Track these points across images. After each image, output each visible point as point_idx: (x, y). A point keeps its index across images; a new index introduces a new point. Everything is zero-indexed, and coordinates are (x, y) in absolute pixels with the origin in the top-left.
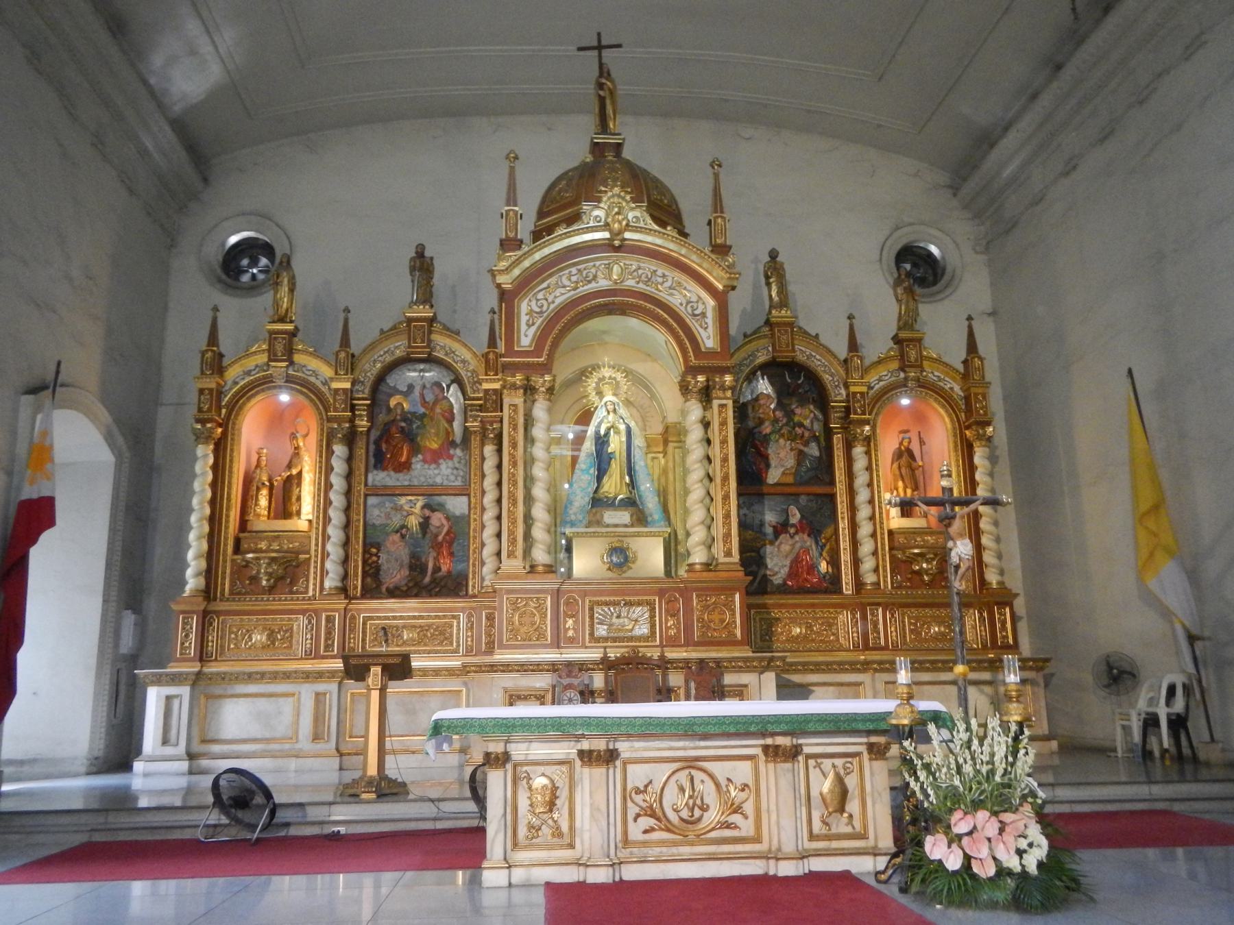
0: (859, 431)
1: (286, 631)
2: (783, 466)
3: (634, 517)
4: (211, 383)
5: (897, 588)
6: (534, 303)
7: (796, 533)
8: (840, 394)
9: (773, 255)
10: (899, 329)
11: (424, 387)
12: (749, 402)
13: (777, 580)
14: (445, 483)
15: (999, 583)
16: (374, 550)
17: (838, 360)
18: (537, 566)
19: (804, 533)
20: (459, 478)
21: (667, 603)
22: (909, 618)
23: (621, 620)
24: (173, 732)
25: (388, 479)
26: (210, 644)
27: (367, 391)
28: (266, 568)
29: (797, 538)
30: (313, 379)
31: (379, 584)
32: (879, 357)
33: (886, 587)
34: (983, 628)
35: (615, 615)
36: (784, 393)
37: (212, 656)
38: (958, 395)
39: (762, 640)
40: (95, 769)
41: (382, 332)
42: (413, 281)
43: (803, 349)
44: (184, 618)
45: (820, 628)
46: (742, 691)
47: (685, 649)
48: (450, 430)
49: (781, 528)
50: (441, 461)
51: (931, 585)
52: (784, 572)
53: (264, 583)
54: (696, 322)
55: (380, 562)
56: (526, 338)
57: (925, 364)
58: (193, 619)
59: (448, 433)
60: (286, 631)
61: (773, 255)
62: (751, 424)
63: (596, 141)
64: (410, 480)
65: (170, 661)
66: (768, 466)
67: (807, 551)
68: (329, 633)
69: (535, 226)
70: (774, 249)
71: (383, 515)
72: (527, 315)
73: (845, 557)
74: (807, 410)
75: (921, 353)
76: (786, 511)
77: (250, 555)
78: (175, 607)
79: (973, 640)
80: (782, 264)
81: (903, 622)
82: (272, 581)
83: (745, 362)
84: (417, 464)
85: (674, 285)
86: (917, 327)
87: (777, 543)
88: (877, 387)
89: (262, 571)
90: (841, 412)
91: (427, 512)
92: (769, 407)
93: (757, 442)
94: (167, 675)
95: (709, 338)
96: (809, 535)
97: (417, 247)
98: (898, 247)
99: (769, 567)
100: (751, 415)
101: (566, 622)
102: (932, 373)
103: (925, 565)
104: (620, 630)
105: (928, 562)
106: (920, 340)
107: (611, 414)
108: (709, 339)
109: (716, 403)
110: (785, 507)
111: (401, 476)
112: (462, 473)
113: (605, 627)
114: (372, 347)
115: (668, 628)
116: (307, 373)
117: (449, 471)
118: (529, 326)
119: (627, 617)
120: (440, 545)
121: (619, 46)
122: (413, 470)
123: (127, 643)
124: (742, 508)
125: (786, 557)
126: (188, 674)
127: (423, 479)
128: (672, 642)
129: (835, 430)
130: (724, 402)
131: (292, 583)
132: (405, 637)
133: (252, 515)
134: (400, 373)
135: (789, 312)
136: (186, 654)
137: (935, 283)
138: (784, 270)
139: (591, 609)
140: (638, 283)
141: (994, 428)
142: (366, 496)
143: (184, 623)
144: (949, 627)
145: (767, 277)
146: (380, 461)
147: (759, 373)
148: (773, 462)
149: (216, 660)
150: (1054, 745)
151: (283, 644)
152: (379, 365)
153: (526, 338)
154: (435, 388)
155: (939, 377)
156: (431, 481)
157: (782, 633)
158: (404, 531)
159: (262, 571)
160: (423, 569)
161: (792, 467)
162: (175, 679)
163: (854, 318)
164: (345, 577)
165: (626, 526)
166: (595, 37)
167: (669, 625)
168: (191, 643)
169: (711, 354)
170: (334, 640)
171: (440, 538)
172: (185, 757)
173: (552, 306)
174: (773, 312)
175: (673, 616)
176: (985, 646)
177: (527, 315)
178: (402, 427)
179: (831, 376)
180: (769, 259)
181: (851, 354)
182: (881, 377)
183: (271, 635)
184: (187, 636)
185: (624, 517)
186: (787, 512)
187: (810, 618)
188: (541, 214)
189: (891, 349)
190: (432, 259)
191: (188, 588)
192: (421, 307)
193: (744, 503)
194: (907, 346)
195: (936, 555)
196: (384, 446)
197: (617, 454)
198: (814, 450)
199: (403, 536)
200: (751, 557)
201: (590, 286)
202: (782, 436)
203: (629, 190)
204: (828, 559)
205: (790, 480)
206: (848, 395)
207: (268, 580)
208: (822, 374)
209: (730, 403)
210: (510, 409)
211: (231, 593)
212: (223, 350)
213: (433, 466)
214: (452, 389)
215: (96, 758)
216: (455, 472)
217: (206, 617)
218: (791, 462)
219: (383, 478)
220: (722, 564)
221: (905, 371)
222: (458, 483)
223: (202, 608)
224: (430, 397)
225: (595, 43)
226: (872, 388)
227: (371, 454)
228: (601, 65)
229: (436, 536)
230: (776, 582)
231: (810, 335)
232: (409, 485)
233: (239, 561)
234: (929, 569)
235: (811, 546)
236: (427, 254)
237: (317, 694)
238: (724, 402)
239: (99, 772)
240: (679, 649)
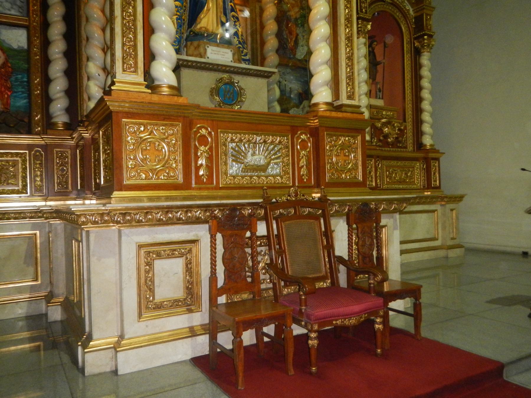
3: (236, 57)
51: (393, 145)
87: (302, 106)
101: (197, 158)
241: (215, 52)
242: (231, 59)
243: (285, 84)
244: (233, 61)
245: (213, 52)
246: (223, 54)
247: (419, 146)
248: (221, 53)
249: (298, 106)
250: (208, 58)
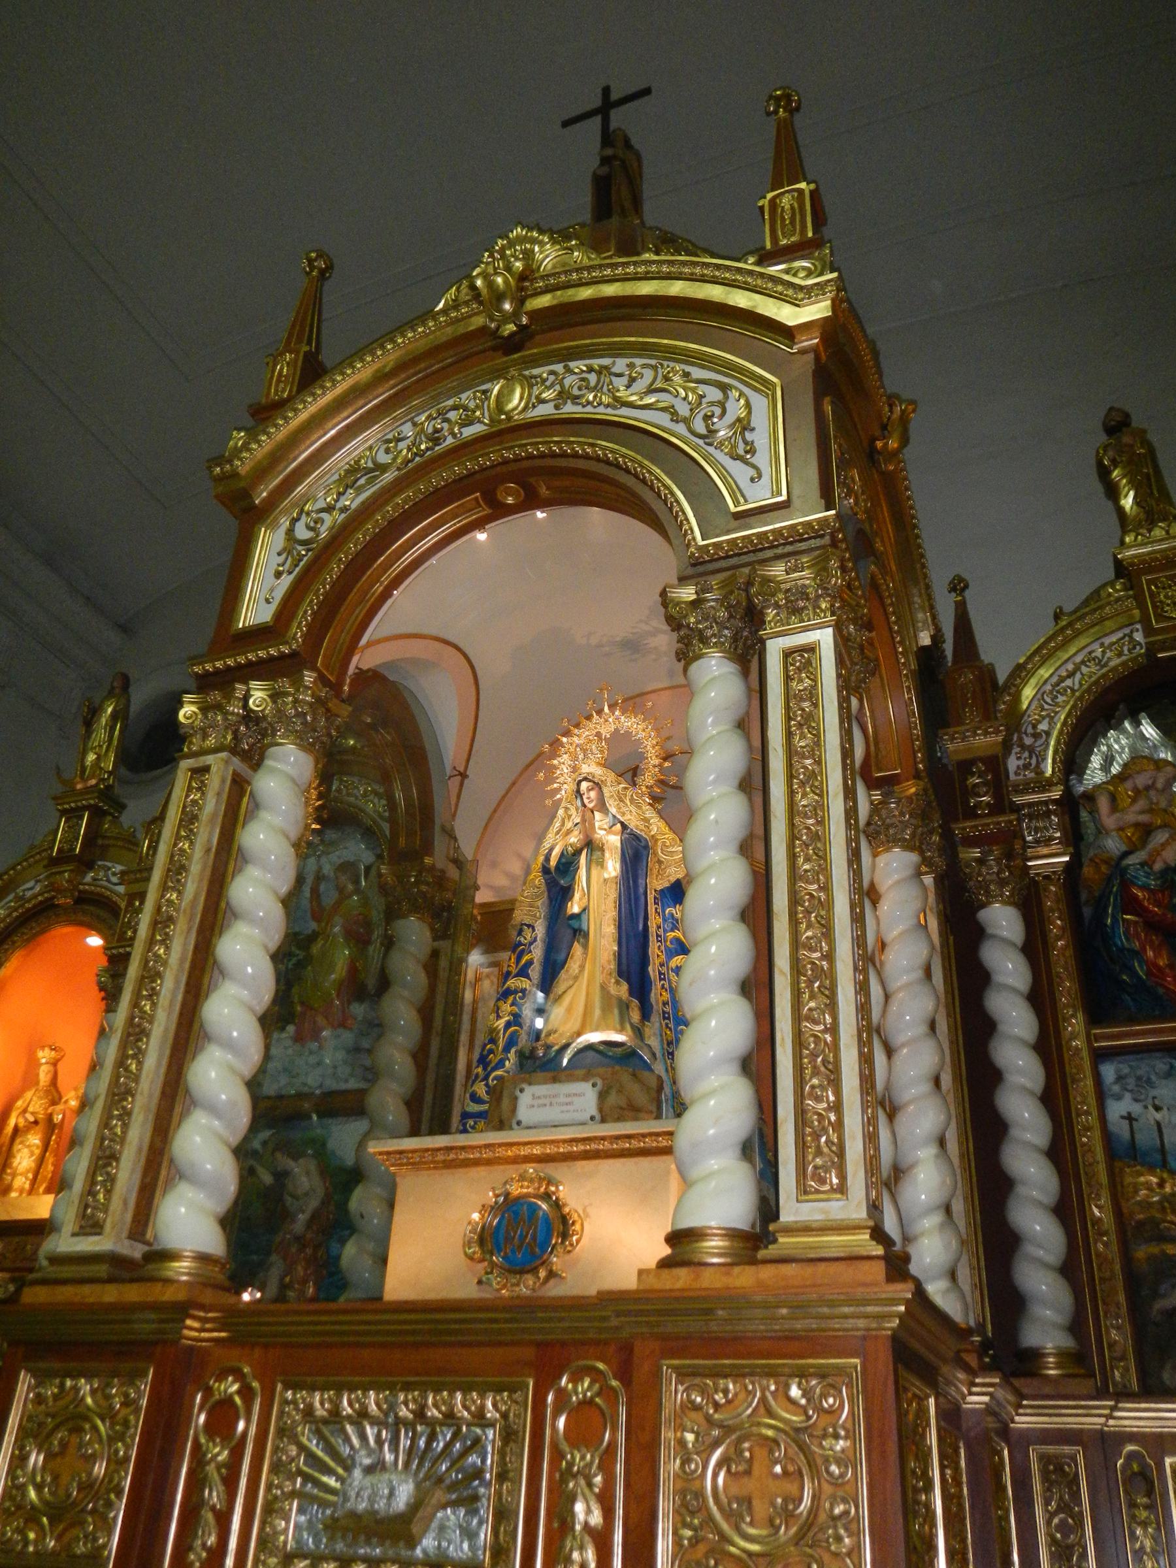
12: (1097, 787)
62: (1113, 845)
100: (1109, 821)
109: (775, 648)
124: (1119, 1098)
127: (283, 1080)
145: (1104, 473)
177: (279, 554)
193: (1120, 1078)
209: (825, 638)
220: (790, 1230)
241: (541, 1102)
242: (593, 1111)
243: (1159, 1124)
244: (598, 1117)
245: (536, 1102)
246: (568, 1100)
248: (562, 1099)
250: (519, 1123)
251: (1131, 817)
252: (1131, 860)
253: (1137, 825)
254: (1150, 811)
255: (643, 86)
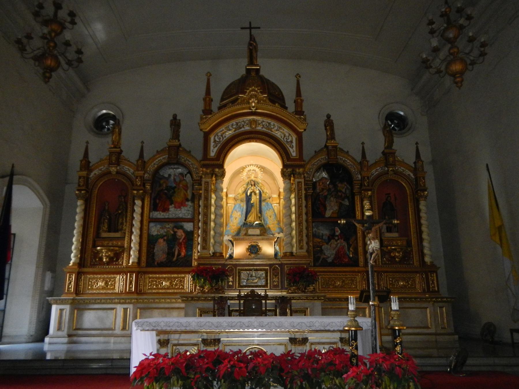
0: (366, 194)
1: (113, 281)
2: (333, 209)
3: (262, 232)
4: (84, 173)
5: (384, 264)
6: (216, 137)
7: (338, 239)
8: (358, 177)
9: (329, 116)
10: (385, 148)
11: (175, 175)
13: (330, 260)
14: (184, 217)
15: (431, 262)
16: (152, 246)
17: (357, 162)
18: (217, 253)
19: (341, 239)
20: (189, 215)
21: (273, 270)
22: (389, 278)
23: (253, 278)
24: (63, 325)
25: (159, 215)
26: (80, 286)
27: (150, 177)
28: (105, 254)
29: (339, 241)
30: (128, 172)
31: (153, 260)
32: (376, 161)
33: (379, 264)
34: (423, 283)
35: (250, 275)
36: (333, 177)
37: (81, 292)
38: (412, 177)
39: (322, 287)
40: (31, 340)
41: (157, 151)
42: (171, 130)
43: (341, 157)
44: (69, 275)
45: (348, 282)
46: (306, 311)
47: (280, 291)
48: (186, 194)
49: (332, 237)
50: (182, 207)
52: (332, 257)
53: (104, 260)
54: (288, 145)
55: (155, 251)
56: (213, 153)
57: (397, 163)
58: (73, 275)
59: (185, 195)
60: (113, 281)
61: (329, 116)
62: (318, 191)
63: (247, 67)
64: (168, 216)
65: (62, 294)
66: (325, 209)
67: (343, 247)
68: (131, 283)
69: (220, 105)
70: (328, 114)
71: (156, 230)
72: (213, 142)
73: (360, 249)
74: (344, 185)
75: (395, 158)
76: (334, 231)
77: (99, 248)
78: (65, 270)
79: (419, 288)
80: (332, 121)
81: (387, 280)
82: (108, 259)
83: (315, 164)
84: (172, 208)
85: (278, 129)
86: (393, 148)
87: (330, 244)
88: (375, 174)
89: (104, 255)
90: (359, 185)
91: (176, 230)
92: (326, 183)
93: (321, 199)
94: (60, 300)
95: (294, 151)
96: (344, 240)
97: (173, 116)
98: (387, 112)
99: (326, 254)
102: (400, 168)
103: (397, 254)
104: (252, 282)
105: (398, 252)
106: (394, 153)
107: (253, 186)
108: (293, 152)
110: (333, 228)
111: (164, 214)
112: (191, 213)
113: (245, 281)
114: (153, 158)
115: (273, 282)
116: (125, 169)
117: (185, 211)
118: (214, 148)
119: (255, 277)
120: (181, 243)
121: (259, 28)
122: (171, 211)
123: (47, 286)
125: (334, 249)
126: (69, 299)
127: (174, 215)
128: (275, 287)
129: (356, 194)
130: (300, 180)
131: (117, 260)
132: (164, 284)
133: (101, 231)
134: (165, 169)
135: (335, 142)
136: (70, 291)
137: (404, 128)
138: (333, 123)
139: (239, 273)
140: (262, 128)
141: (428, 192)
142: (149, 222)
143: (70, 277)
144: (408, 282)
145: (326, 126)
146: (154, 207)
147: (322, 169)
148: (328, 208)
149: (83, 294)
150: (456, 337)
151: (111, 286)
152: (156, 166)
153: (213, 153)
154: (180, 175)
155: (403, 169)
156: (177, 216)
157: (331, 284)
158: (165, 238)
159: (104, 255)
160: (173, 255)
161: (337, 210)
162: (63, 302)
163: (364, 144)
164: (139, 258)
165: (258, 235)
166: (249, 24)
167: (274, 280)
168: (72, 286)
169: (295, 160)
170: (132, 286)
171: (181, 241)
172: (66, 336)
173: (225, 139)
174: (328, 141)
175: (276, 276)
176: (424, 290)
177: (213, 142)
178: (165, 193)
179: (354, 169)
180: (327, 118)
181: (363, 160)
182: (377, 170)
183: (106, 283)
184: (70, 283)
185: (257, 231)
186: (334, 230)
187: (344, 278)
188: (222, 99)
189: (381, 157)
190: (180, 120)
191: (72, 262)
192: (174, 141)
193: (315, 225)
194: (389, 156)
195: (401, 249)
196: (158, 201)
197: (255, 204)
198: (346, 203)
199: (164, 240)
200: (318, 249)
201: (241, 130)
202: (332, 196)
203: (259, 88)
204: (353, 251)
205: (335, 215)
206: (361, 178)
207: (106, 259)
208: (350, 168)
209: (303, 180)
210: (205, 184)
211: (91, 264)
212: (90, 160)
213: (178, 209)
214: (187, 176)
215: (31, 336)
216: (188, 212)
217: (79, 275)
218: (336, 208)
219: (157, 215)
221: (388, 167)
222: (189, 217)
223: (77, 270)
224: (178, 180)
225: (248, 26)
226: (373, 175)
227: (152, 204)
228: (251, 35)
229: (180, 239)
230: (329, 261)
231: (344, 151)
232: (168, 218)
233: (94, 250)
234: (398, 256)
235: (345, 245)
236: (178, 118)
237: (124, 309)
238: (300, 180)
239: (32, 342)
240: (278, 291)
247: (423, 262)
249: (327, 243)
251: (322, 187)
252: (320, 194)
253: (322, 188)
254: (324, 186)
255: (259, 26)
